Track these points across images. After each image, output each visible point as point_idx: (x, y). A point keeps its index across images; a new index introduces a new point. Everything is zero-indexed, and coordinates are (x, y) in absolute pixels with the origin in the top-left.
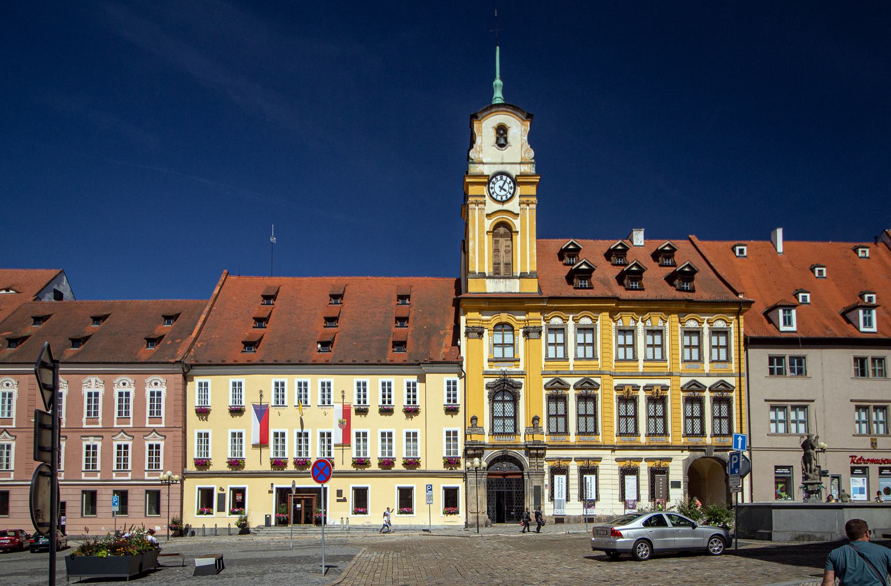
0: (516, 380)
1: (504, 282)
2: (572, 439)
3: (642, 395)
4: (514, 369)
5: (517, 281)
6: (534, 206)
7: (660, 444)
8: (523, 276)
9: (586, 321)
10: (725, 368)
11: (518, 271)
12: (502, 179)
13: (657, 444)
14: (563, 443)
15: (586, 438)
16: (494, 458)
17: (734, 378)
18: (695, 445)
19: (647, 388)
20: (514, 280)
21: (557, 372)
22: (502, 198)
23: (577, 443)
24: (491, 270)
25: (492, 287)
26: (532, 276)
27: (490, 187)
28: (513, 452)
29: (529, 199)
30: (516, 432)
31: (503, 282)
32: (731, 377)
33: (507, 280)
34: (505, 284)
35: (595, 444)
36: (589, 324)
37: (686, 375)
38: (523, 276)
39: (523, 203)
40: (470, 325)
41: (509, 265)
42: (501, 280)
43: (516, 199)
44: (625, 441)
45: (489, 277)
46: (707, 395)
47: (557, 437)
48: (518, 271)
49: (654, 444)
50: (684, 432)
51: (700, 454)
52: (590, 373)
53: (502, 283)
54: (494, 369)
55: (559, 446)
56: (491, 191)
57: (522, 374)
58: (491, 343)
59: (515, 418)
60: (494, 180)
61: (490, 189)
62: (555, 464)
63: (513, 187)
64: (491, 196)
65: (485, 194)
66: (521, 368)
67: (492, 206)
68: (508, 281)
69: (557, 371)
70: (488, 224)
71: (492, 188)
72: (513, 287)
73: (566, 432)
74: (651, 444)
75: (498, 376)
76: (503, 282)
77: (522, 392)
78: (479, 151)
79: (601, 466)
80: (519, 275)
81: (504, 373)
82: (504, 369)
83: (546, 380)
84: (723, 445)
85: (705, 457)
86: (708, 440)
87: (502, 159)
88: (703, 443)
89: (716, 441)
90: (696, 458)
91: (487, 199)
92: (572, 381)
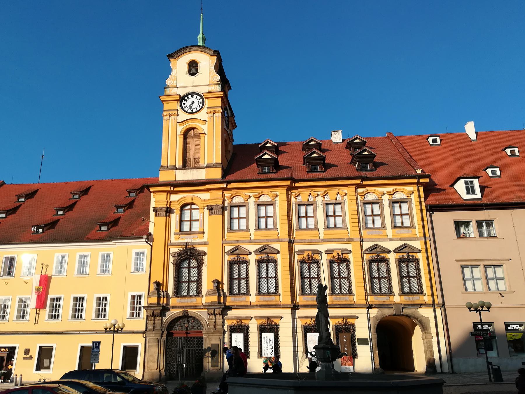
0: (200, 249)
1: (192, 171)
2: (253, 299)
3: (324, 259)
4: (198, 240)
5: (204, 171)
6: (220, 114)
7: (344, 303)
8: (208, 166)
9: (264, 199)
10: (408, 233)
11: (204, 162)
12: (193, 97)
13: (340, 303)
14: (242, 304)
15: (266, 298)
16: (174, 318)
17: (419, 241)
18: (382, 303)
19: (329, 252)
20: (201, 169)
21: (237, 241)
22: (192, 111)
23: (258, 303)
24: (181, 164)
25: (182, 176)
26: (216, 166)
27: (183, 103)
28: (192, 312)
29: (214, 109)
30: (199, 293)
31: (190, 172)
32: (415, 240)
33: (194, 170)
34: (193, 173)
35: (274, 303)
36: (268, 201)
37: (368, 240)
38: (208, 166)
39: (211, 112)
40: (158, 206)
41: (197, 160)
42: (189, 170)
43: (205, 110)
44: (307, 301)
45: (179, 169)
46: (392, 257)
47: (237, 298)
48: (204, 162)
49: (337, 303)
50: (369, 292)
51: (387, 312)
52: (269, 241)
53: (189, 173)
54: (180, 241)
55: (237, 306)
56: (183, 106)
57: (205, 244)
58: (177, 220)
59: (199, 281)
60: (186, 98)
61: (183, 105)
62: (233, 323)
63: (202, 102)
64: (183, 109)
65: (178, 109)
66: (205, 239)
67: (183, 116)
68: (195, 171)
69: (237, 241)
70: (181, 129)
71: (184, 104)
72: (200, 175)
73: (248, 294)
74: (335, 303)
75: (181, 247)
76: (190, 172)
77: (205, 258)
78: (174, 79)
79: (281, 323)
80: (205, 166)
81: (187, 244)
82: (189, 240)
83: (227, 248)
84: (412, 303)
85: (394, 315)
86: (397, 299)
87: (193, 83)
88: (390, 301)
89: (404, 299)
90: (385, 315)
91: (180, 112)
92: (252, 248)
